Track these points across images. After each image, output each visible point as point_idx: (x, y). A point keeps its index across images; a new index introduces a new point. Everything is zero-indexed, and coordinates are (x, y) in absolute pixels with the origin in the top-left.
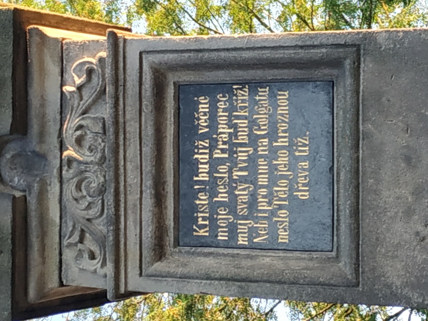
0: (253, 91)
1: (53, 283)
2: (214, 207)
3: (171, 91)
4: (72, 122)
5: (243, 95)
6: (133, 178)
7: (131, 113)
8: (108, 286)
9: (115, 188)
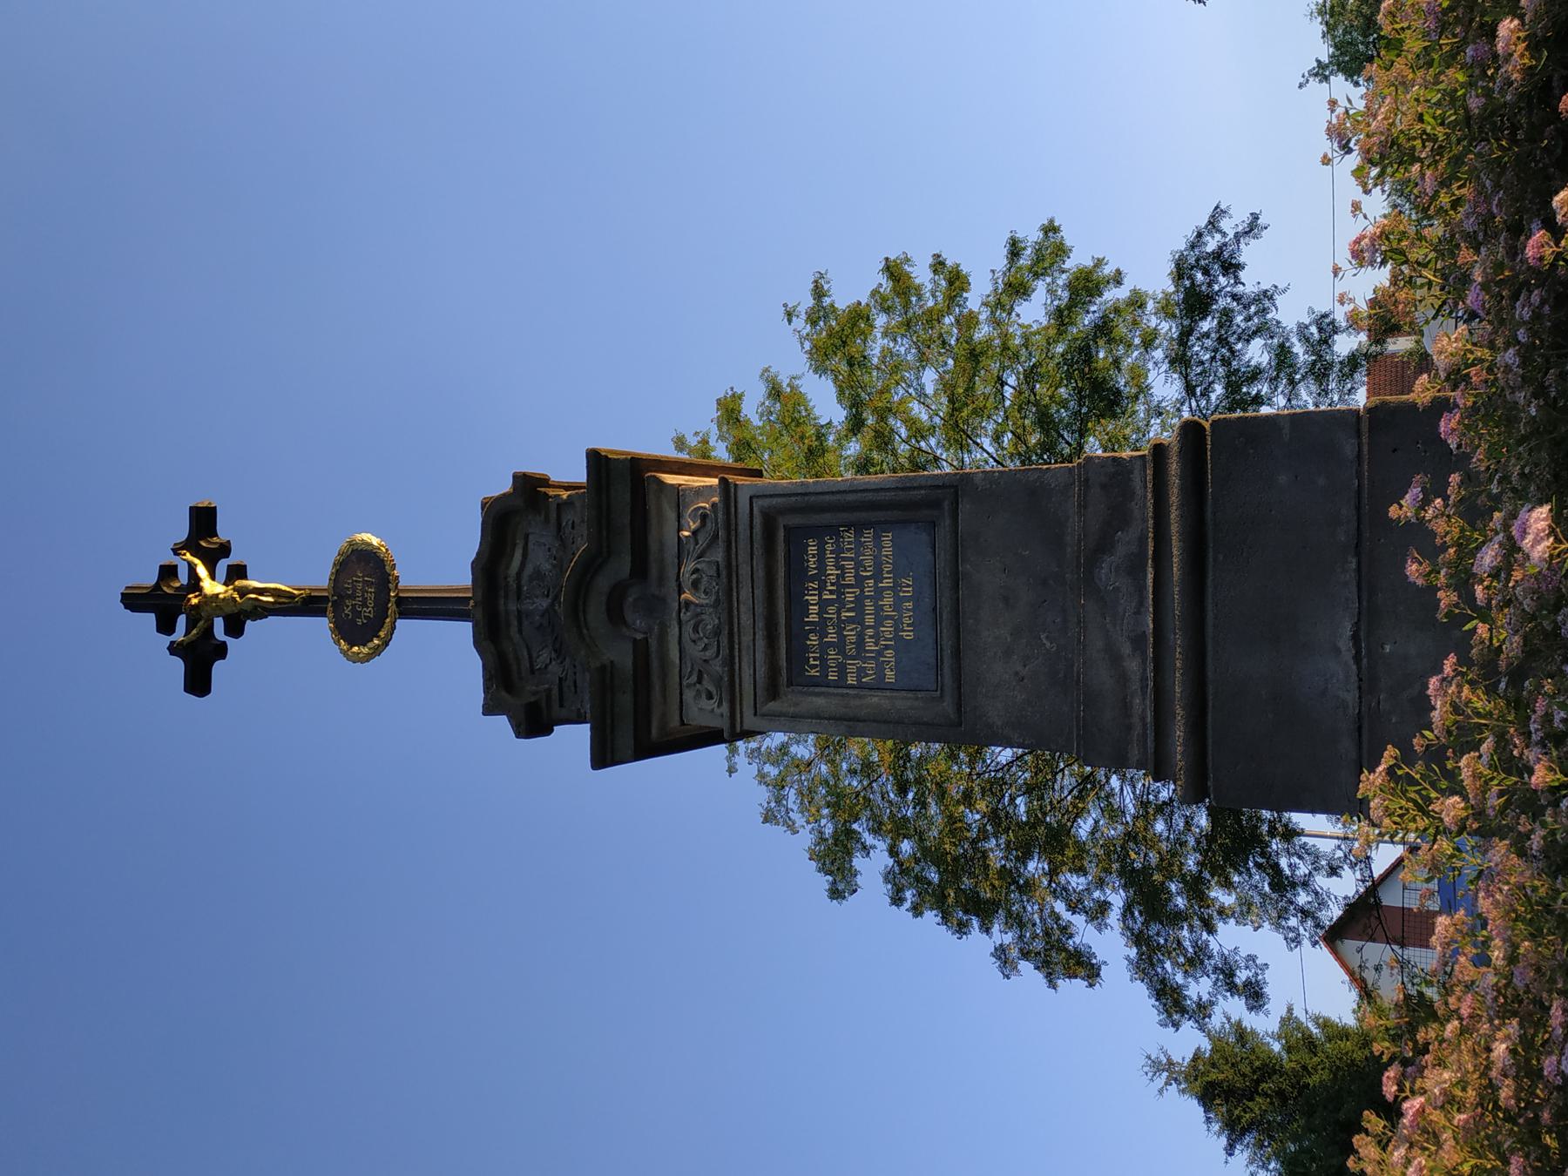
0: (859, 534)
1: (674, 722)
2: (824, 647)
3: (781, 534)
4: (689, 566)
5: (849, 537)
6: (746, 619)
7: (743, 555)
8: (722, 723)
9: (729, 629)
